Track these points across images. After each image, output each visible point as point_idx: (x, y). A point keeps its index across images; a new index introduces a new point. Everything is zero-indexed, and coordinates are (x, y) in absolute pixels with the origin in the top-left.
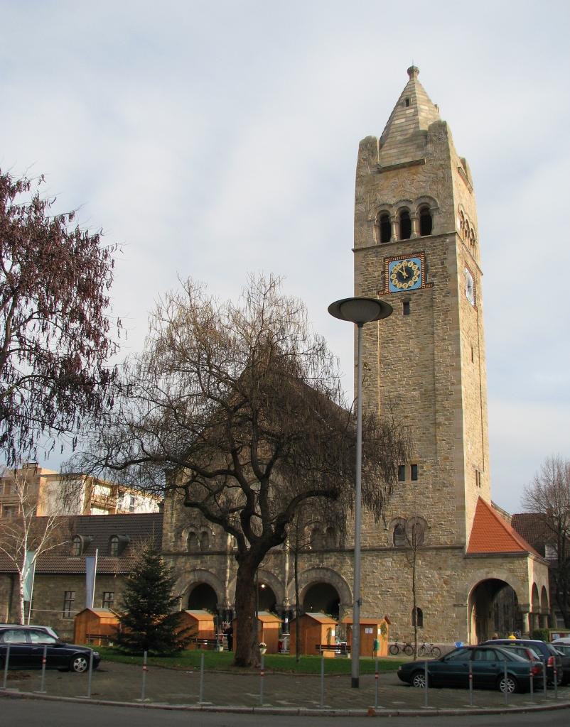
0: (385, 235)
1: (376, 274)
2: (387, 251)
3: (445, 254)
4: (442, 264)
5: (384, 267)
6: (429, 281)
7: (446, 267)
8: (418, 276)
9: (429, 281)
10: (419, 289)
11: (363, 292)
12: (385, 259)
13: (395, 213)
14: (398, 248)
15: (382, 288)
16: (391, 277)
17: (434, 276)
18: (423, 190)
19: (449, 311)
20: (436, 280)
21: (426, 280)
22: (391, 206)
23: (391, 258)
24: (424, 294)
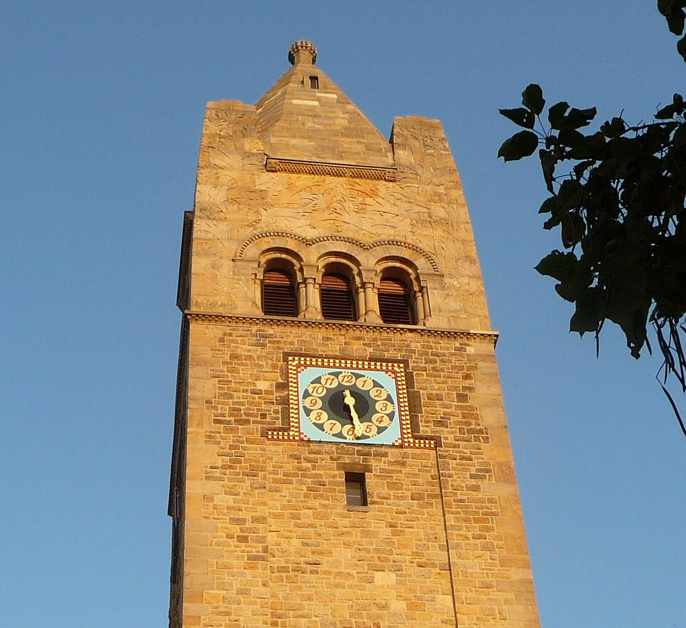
0: (280, 299)
1: (262, 385)
2: (289, 336)
3: (467, 377)
4: (462, 397)
5: (285, 374)
6: (425, 429)
7: (472, 408)
8: (391, 416)
9: (425, 429)
10: (393, 446)
11: (217, 421)
12: (286, 355)
13: (313, 262)
14: (328, 339)
15: (279, 424)
16: (307, 402)
17: (440, 423)
18: (392, 231)
19: (493, 514)
20: (448, 435)
21: (415, 426)
22: (308, 243)
23: (307, 356)
24: (409, 461)
